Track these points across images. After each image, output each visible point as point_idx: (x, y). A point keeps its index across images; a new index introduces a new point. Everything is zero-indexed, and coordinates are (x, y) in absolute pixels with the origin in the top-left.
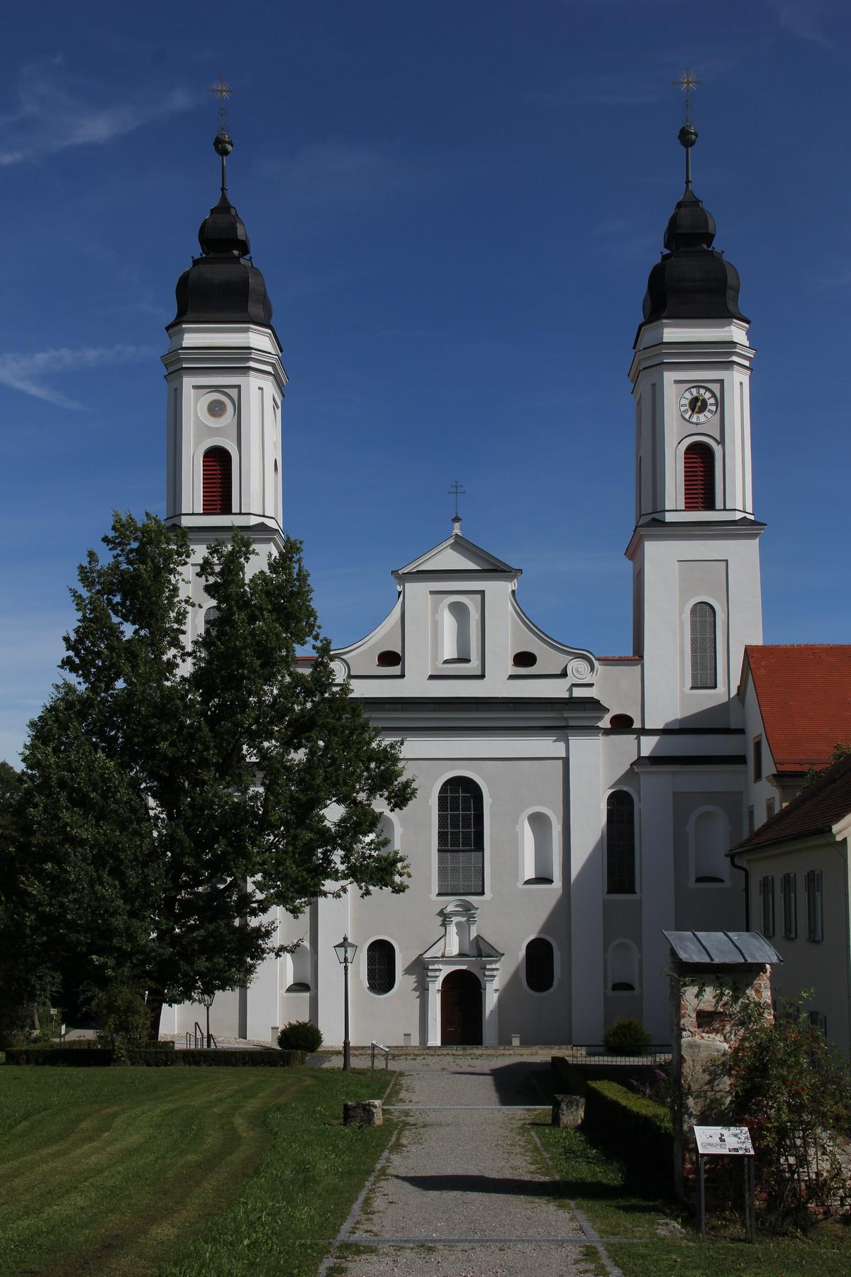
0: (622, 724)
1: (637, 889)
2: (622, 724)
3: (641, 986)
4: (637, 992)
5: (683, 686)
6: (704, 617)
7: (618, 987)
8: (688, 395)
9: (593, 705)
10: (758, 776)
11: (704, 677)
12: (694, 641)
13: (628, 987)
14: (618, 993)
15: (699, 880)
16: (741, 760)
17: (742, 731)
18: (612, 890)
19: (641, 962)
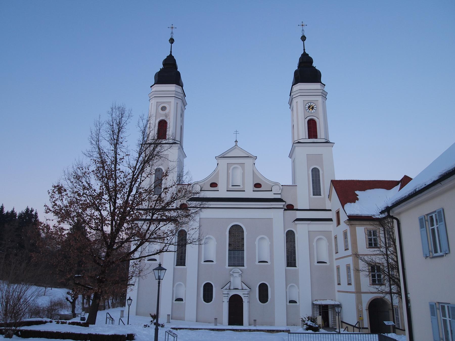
0: (290, 207)
1: (297, 265)
2: (290, 207)
3: (299, 302)
4: (298, 304)
5: (309, 194)
6: (316, 173)
7: (291, 302)
8: (308, 105)
9: (280, 200)
10: (339, 223)
11: (317, 191)
12: (313, 180)
13: (295, 302)
14: (291, 304)
15: (318, 262)
16: (331, 220)
17: (330, 210)
18: (288, 266)
19: (299, 292)
